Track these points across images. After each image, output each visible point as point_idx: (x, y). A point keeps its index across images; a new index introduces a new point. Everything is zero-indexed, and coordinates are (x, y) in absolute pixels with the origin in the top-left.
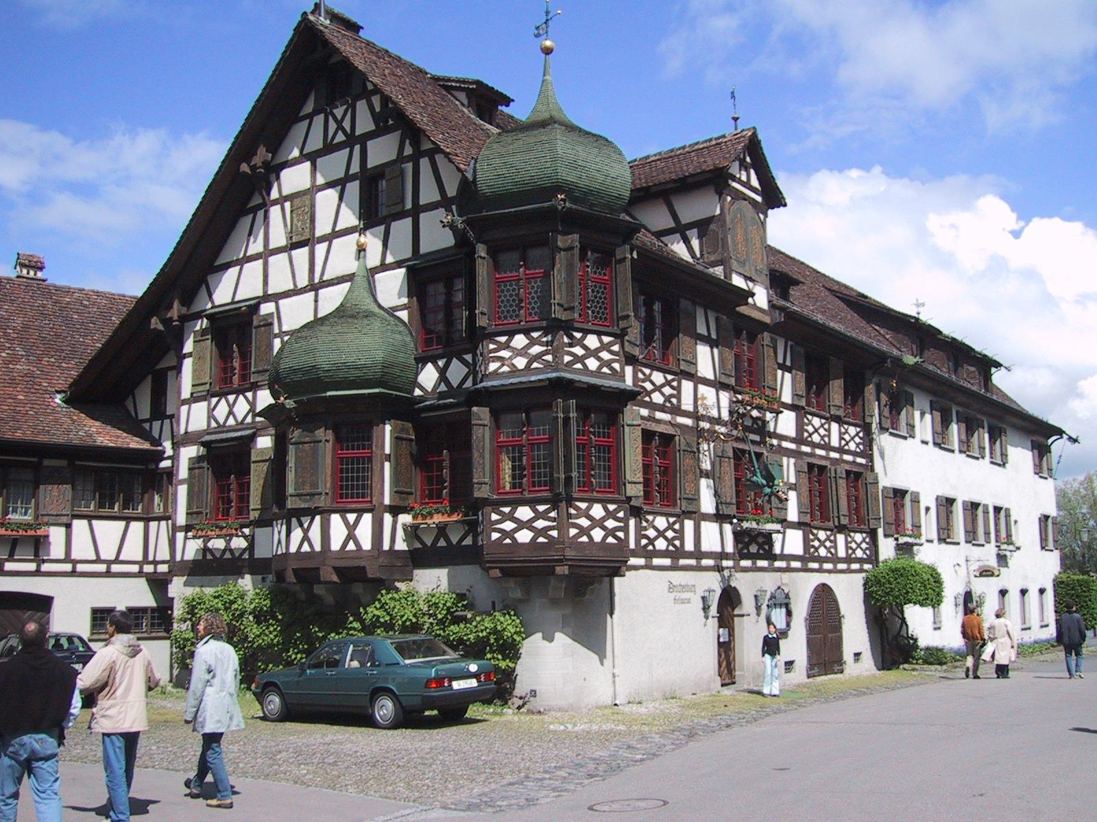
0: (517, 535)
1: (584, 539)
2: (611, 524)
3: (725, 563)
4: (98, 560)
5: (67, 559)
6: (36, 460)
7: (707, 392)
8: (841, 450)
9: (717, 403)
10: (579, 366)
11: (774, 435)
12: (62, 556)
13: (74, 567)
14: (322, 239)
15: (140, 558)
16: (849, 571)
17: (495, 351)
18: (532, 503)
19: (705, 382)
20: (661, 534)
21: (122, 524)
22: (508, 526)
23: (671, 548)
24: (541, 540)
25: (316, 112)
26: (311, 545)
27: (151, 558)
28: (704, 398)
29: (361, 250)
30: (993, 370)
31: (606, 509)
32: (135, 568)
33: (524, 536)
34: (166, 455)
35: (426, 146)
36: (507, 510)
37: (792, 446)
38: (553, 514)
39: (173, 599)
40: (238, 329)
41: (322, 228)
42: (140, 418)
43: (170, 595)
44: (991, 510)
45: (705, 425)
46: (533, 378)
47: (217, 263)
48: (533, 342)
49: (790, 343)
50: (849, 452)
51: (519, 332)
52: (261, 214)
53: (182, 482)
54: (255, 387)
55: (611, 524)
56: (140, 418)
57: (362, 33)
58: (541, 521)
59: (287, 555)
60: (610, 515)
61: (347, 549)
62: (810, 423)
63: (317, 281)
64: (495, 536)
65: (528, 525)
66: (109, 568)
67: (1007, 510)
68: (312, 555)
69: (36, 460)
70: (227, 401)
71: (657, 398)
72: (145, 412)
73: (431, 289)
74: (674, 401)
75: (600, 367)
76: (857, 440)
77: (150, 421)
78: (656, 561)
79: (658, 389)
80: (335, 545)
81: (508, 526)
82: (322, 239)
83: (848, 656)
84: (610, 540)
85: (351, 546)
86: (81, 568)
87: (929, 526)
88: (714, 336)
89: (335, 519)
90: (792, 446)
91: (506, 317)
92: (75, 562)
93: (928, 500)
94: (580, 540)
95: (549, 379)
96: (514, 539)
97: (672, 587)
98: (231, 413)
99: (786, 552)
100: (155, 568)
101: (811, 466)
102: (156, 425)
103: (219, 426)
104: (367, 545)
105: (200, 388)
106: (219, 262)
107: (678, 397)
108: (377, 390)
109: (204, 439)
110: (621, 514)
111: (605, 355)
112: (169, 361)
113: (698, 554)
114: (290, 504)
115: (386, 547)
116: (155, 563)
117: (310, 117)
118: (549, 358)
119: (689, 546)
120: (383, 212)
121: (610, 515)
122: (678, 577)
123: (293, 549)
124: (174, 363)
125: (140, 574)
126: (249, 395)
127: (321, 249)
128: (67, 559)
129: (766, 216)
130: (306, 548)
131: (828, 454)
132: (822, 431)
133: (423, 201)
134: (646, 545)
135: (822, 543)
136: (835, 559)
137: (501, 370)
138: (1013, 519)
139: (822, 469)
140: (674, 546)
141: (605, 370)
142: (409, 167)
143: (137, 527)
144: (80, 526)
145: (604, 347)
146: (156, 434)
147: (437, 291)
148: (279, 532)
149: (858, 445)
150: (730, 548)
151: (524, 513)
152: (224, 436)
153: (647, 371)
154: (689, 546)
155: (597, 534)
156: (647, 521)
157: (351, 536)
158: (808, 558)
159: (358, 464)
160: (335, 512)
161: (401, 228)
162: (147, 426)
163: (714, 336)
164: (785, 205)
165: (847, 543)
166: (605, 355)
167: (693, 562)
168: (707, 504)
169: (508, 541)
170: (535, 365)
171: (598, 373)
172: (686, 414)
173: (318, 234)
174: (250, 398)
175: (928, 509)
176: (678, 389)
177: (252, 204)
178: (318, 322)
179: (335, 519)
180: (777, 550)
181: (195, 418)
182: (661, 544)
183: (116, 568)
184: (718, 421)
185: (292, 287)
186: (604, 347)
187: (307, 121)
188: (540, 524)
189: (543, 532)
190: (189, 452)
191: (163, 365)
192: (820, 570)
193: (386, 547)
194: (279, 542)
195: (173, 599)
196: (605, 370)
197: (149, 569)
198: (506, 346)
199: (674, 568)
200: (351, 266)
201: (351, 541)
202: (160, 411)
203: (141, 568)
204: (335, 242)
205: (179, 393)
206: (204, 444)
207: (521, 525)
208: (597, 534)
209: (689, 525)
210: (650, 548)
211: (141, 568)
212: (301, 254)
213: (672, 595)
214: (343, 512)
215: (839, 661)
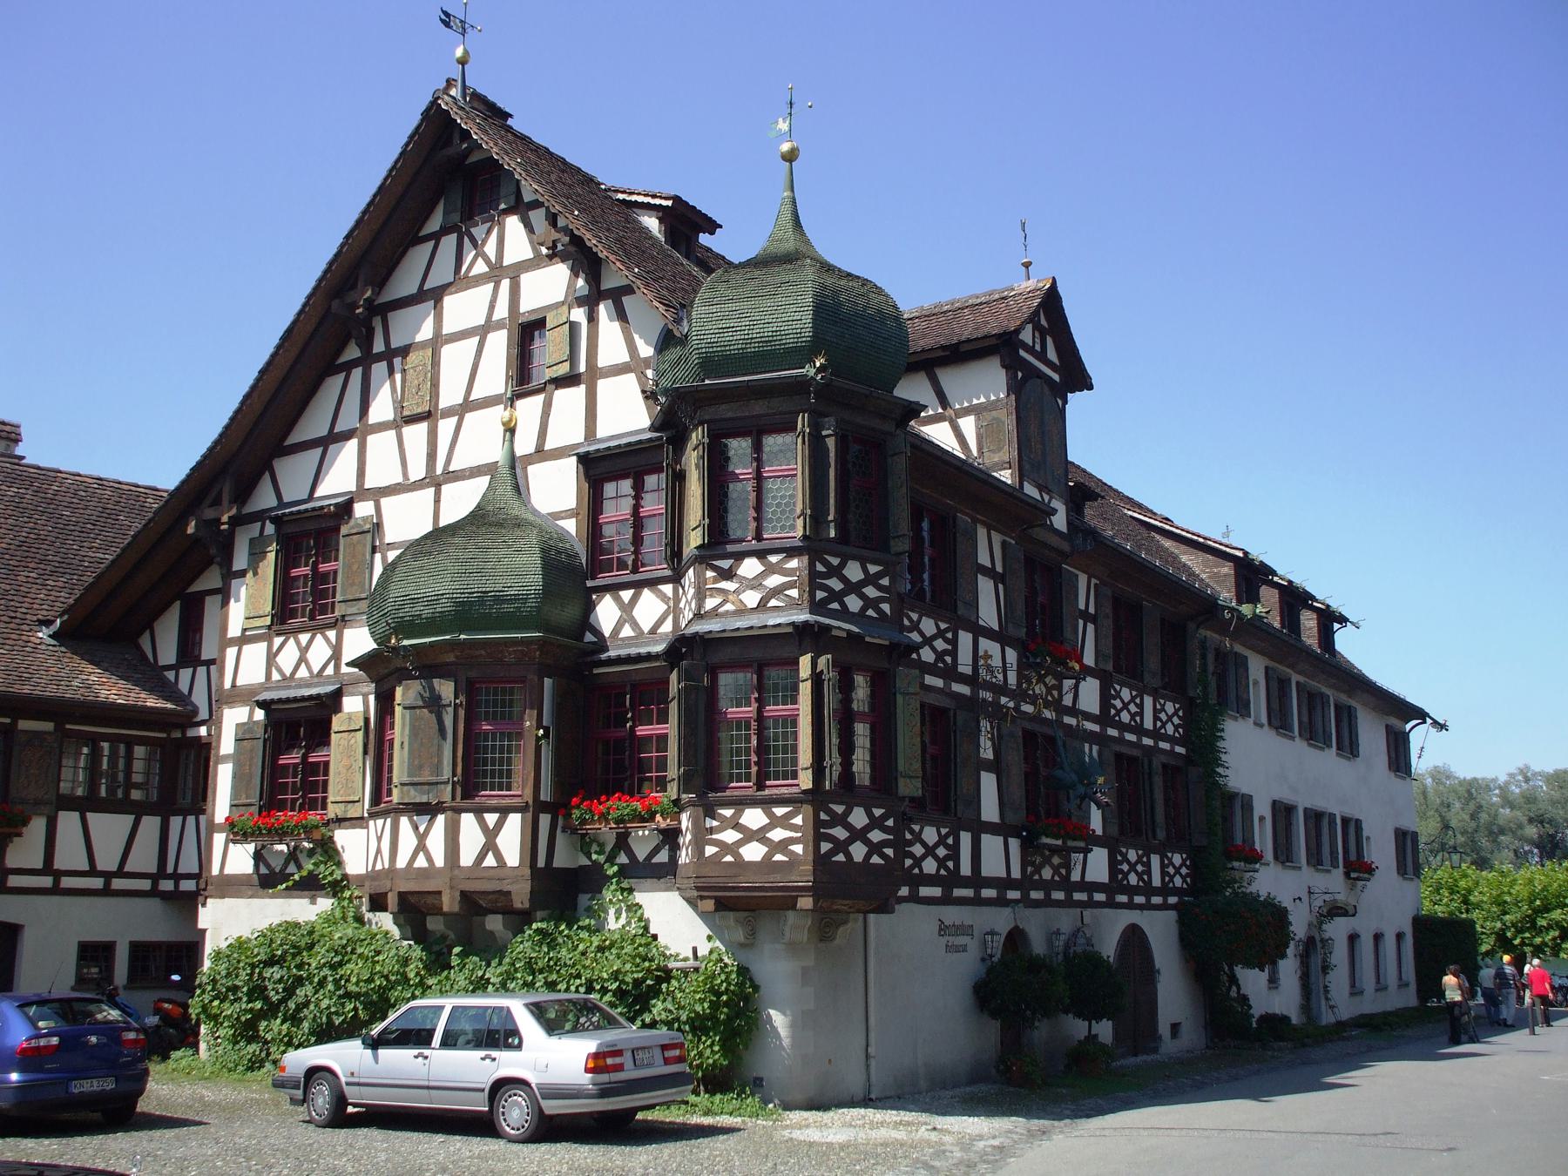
0: (742, 850)
1: (841, 857)
2: (876, 836)
3: (1013, 895)
4: (93, 872)
5: (48, 868)
6: (8, 721)
7: (989, 646)
8: (1156, 734)
9: (1001, 659)
10: (835, 606)
11: (1073, 711)
12: (39, 865)
13: (57, 882)
14: (448, 413)
15: (152, 868)
16: (1164, 907)
18: (767, 803)
19: (989, 633)
20: (930, 851)
21: (129, 819)
22: (730, 836)
23: (943, 872)
24: (779, 857)
25: (445, 230)
26: (429, 859)
27: (170, 870)
28: (987, 656)
29: (510, 430)
30: (1336, 626)
31: (870, 814)
32: (146, 885)
33: (753, 852)
34: (198, 719)
35: (607, 284)
37: (1096, 728)
38: (798, 820)
39: (204, 931)
40: (315, 536)
41: (450, 395)
42: (161, 663)
43: (201, 925)
44: (1339, 821)
45: (987, 695)
46: (772, 621)
47: (287, 443)
48: (771, 570)
49: (1094, 581)
50: (1166, 738)
52: (357, 373)
53: (226, 758)
54: (341, 623)
55: (876, 836)
56: (161, 663)
57: (510, 122)
58: (778, 830)
59: (392, 871)
60: (875, 823)
62: (1118, 696)
63: (439, 471)
64: (710, 850)
65: (759, 835)
66: (107, 884)
67: (1358, 823)
69: (8, 721)
70: (298, 643)
71: (927, 655)
72: (168, 653)
73: (609, 489)
74: (948, 659)
75: (864, 609)
76: (1176, 720)
77: (176, 667)
78: (925, 891)
79: (928, 641)
80: (467, 858)
81: (730, 836)
82: (448, 413)
83: (1164, 1029)
84: (876, 859)
85: (490, 861)
86: (67, 882)
87: (1263, 840)
88: (999, 569)
89: (468, 820)
90: (1096, 728)
92: (58, 875)
93: (1262, 808)
95: (793, 624)
96: (738, 856)
97: (943, 929)
98: (302, 659)
99: (1088, 878)
100: (177, 885)
101: (1119, 757)
102: (186, 674)
103: (285, 678)
105: (258, 623)
106: (290, 441)
107: (954, 653)
109: (261, 697)
110: (890, 823)
111: (871, 592)
112: (211, 579)
113: (977, 881)
115: (541, 863)
116: (177, 877)
117: (436, 237)
118: (794, 593)
119: (966, 869)
120: (542, 374)
121: (875, 823)
122: (952, 914)
123: (401, 863)
124: (218, 584)
125: (154, 893)
126: (332, 634)
127: (446, 426)
128: (48, 868)
129: (1065, 402)
130: (421, 862)
131: (1140, 739)
132: (1133, 708)
133: (603, 361)
134: (912, 867)
135: (1132, 867)
136: (1148, 890)
137: (721, 610)
138: (1365, 834)
139: (1132, 760)
140: (947, 869)
141: (870, 612)
143: (151, 824)
144: (68, 822)
145: (870, 580)
146: (184, 686)
147: (619, 494)
148: (379, 839)
149: (1176, 727)
150: (1016, 873)
151: (754, 818)
152: (292, 693)
153: (915, 616)
154: (966, 869)
155: (858, 851)
156: (912, 832)
157: (490, 846)
158: (1116, 884)
160: (467, 811)
161: (570, 401)
162: (171, 675)
163: (999, 569)
164: (1090, 387)
165: (1163, 866)
166: (871, 592)
167: (968, 893)
168: (990, 810)
169: (729, 858)
170: (773, 603)
171: (858, 618)
172: (963, 679)
173: (443, 404)
174: (333, 640)
175: (1262, 819)
176: (954, 642)
177: (342, 359)
178: (439, 535)
179: (468, 820)
180: (1076, 876)
181: (247, 666)
182: (930, 866)
183: (117, 884)
184: (1002, 689)
185: (398, 478)
186: (870, 580)
187: (432, 243)
188: (778, 834)
189: (783, 845)
190: (234, 717)
191: (198, 586)
192: (1130, 906)
193: (541, 863)
194: (379, 851)
195: (204, 931)
196: (870, 612)
197: (167, 885)
199: (946, 900)
200: (494, 452)
202: (189, 654)
203: (155, 884)
204: (468, 416)
205: (224, 628)
206: (262, 705)
207: (750, 836)
208: (858, 851)
209: (966, 838)
210: (916, 871)
211: (155, 884)
212: (416, 434)
213: (944, 940)
214: (479, 812)
215: (1155, 1036)
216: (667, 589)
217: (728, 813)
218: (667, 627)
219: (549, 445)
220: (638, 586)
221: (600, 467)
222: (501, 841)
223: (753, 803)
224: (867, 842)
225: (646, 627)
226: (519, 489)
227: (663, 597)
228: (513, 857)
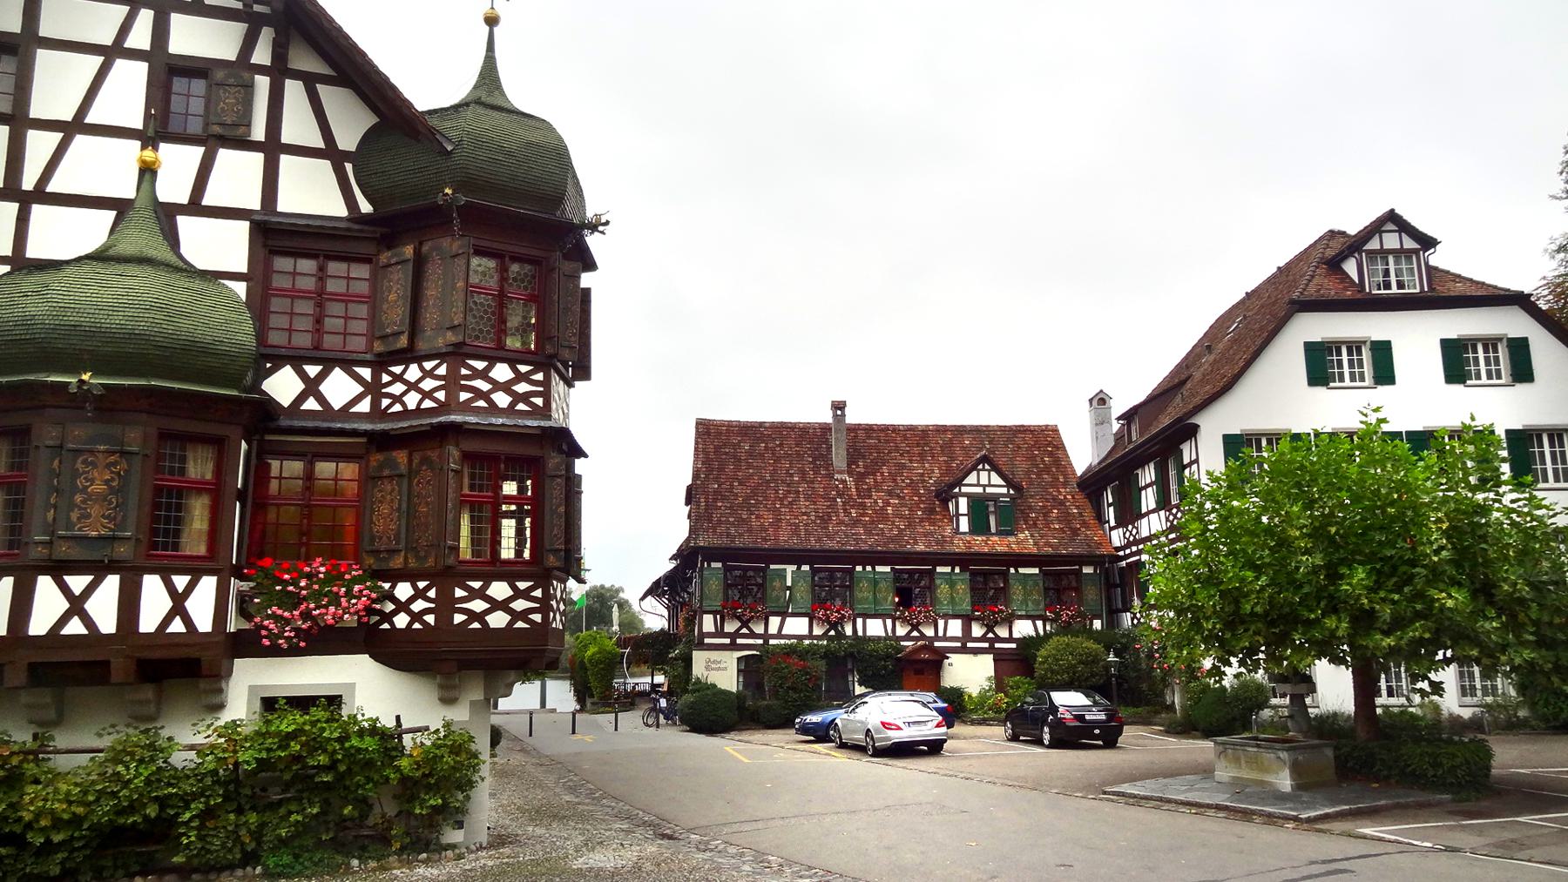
17: (467, 378)
22: (478, 606)
24: (520, 624)
29: (148, 172)
33: (498, 620)
36: (476, 585)
38: (538, 593)
48: (520, 378)
51: (503, 360)
63: (28, 183)
64: (459, 618)
65: (503, 606)
81: (478, 606)
85: (177, 626)
91: (477, 338)
96: (485, 623)
108: (235, 393)
114: (38, 553)
142: (263, 83)
159: (170, 496)
160: (152, 571)
169: (476, 625)
188: (520, 605)
198: (484, 375)
204: (80, 141)
207: (496, 605)
216: (366, 373)
218: (364, 406)
219: (208, 200)
220: (328, 364)
221: (274, 234)
222: (190, 605)
223: (500, 578)
225: (337, 404)
226: (172, 238)
227: (358, 379)
228: (204, 623)
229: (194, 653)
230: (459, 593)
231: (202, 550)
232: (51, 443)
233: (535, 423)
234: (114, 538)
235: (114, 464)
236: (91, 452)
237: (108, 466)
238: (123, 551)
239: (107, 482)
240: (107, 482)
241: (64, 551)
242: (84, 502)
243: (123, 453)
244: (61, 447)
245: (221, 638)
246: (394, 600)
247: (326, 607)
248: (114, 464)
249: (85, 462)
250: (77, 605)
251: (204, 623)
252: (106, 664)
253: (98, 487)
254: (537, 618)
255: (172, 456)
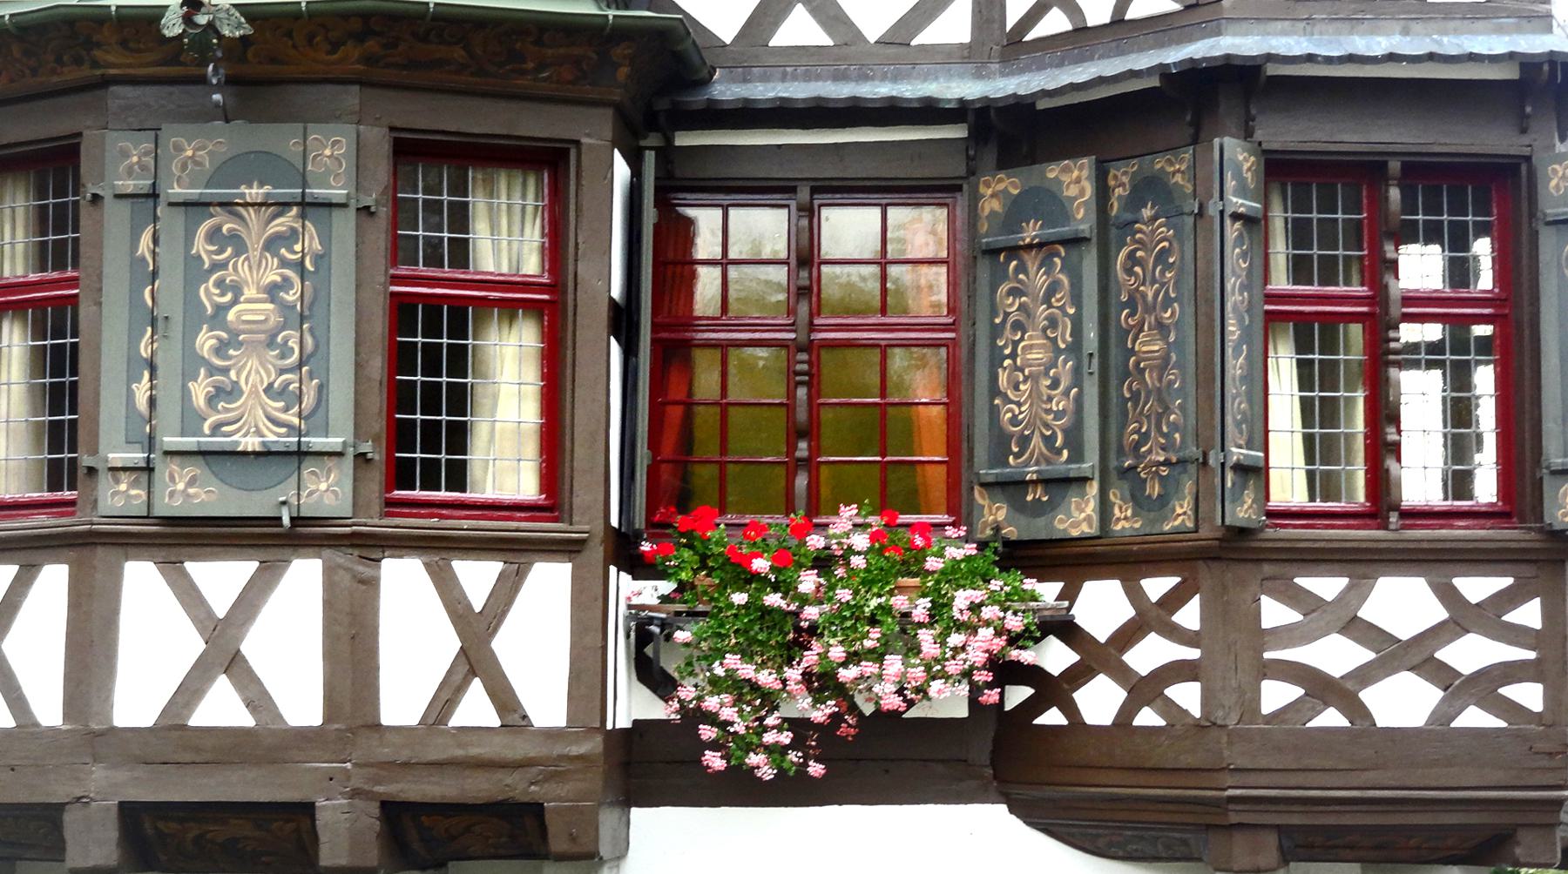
0: (1368, 696)
24: (1474, 717)
33: (1402, 702)
38: (1529, 614)
61: (456, 721)
64: (1276, 695)
65: (1417, 655)
68: (269, 743)
81: (1336, 655)
85: (476, 709)
89: (403, 581)
94: (1316, 722)
96: (1357, 711)
104: (302, 703)
114: (118, 499)
130: (221, 708)
157: (475, 660)
159: (433, 329)
169: (1332, 718)
188: (1470, 653)
201: (477, 685)
207: (1395, 654)
214: (438, 549)
217: (1327, 586)
224: (1122, 674)
225: (873, 26)
228: (548, 707)
229: (517, 786)
230: (1274, 613)
231: (524, 484)
232: (129, 185)
233: (1498, 45)
234: (301, 454)
235: (291, 237)
236: (227, 205)
237: (272, 244)
238: (326, 492)
239: (272, 291)
240: (272, 291)
241: (188, 492)
242: (220, 350)
243: (308, 206)
244: (153, 195)
245: (592, 746)
246: (1067, 630)
247: (878, 656)
248: (291, 237)
249: (214, 235)
250: (223, 653)
251: (548, 707)
252: (308, 809)
253: (252, 310)
254: (1529, 695)
255: (433, 208)
